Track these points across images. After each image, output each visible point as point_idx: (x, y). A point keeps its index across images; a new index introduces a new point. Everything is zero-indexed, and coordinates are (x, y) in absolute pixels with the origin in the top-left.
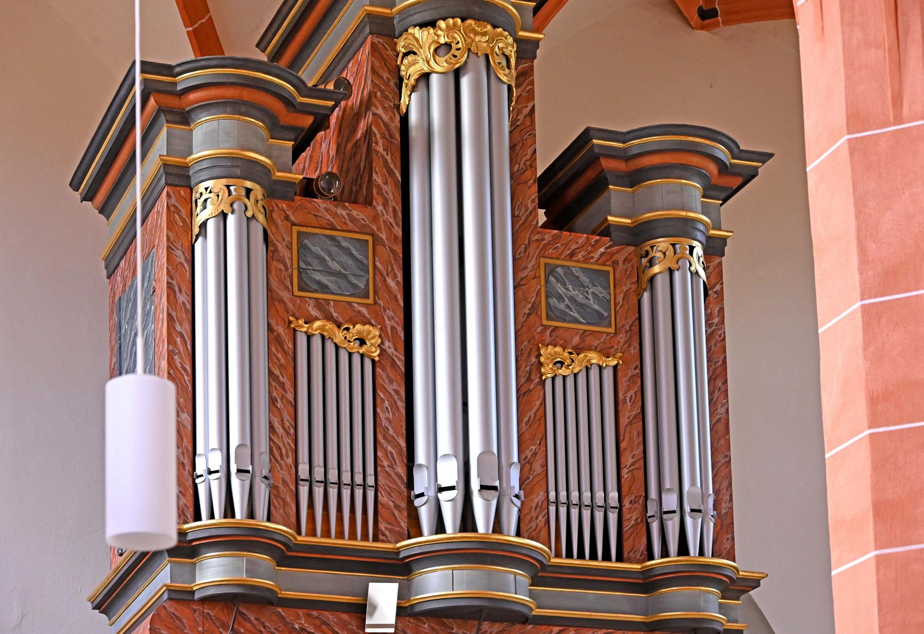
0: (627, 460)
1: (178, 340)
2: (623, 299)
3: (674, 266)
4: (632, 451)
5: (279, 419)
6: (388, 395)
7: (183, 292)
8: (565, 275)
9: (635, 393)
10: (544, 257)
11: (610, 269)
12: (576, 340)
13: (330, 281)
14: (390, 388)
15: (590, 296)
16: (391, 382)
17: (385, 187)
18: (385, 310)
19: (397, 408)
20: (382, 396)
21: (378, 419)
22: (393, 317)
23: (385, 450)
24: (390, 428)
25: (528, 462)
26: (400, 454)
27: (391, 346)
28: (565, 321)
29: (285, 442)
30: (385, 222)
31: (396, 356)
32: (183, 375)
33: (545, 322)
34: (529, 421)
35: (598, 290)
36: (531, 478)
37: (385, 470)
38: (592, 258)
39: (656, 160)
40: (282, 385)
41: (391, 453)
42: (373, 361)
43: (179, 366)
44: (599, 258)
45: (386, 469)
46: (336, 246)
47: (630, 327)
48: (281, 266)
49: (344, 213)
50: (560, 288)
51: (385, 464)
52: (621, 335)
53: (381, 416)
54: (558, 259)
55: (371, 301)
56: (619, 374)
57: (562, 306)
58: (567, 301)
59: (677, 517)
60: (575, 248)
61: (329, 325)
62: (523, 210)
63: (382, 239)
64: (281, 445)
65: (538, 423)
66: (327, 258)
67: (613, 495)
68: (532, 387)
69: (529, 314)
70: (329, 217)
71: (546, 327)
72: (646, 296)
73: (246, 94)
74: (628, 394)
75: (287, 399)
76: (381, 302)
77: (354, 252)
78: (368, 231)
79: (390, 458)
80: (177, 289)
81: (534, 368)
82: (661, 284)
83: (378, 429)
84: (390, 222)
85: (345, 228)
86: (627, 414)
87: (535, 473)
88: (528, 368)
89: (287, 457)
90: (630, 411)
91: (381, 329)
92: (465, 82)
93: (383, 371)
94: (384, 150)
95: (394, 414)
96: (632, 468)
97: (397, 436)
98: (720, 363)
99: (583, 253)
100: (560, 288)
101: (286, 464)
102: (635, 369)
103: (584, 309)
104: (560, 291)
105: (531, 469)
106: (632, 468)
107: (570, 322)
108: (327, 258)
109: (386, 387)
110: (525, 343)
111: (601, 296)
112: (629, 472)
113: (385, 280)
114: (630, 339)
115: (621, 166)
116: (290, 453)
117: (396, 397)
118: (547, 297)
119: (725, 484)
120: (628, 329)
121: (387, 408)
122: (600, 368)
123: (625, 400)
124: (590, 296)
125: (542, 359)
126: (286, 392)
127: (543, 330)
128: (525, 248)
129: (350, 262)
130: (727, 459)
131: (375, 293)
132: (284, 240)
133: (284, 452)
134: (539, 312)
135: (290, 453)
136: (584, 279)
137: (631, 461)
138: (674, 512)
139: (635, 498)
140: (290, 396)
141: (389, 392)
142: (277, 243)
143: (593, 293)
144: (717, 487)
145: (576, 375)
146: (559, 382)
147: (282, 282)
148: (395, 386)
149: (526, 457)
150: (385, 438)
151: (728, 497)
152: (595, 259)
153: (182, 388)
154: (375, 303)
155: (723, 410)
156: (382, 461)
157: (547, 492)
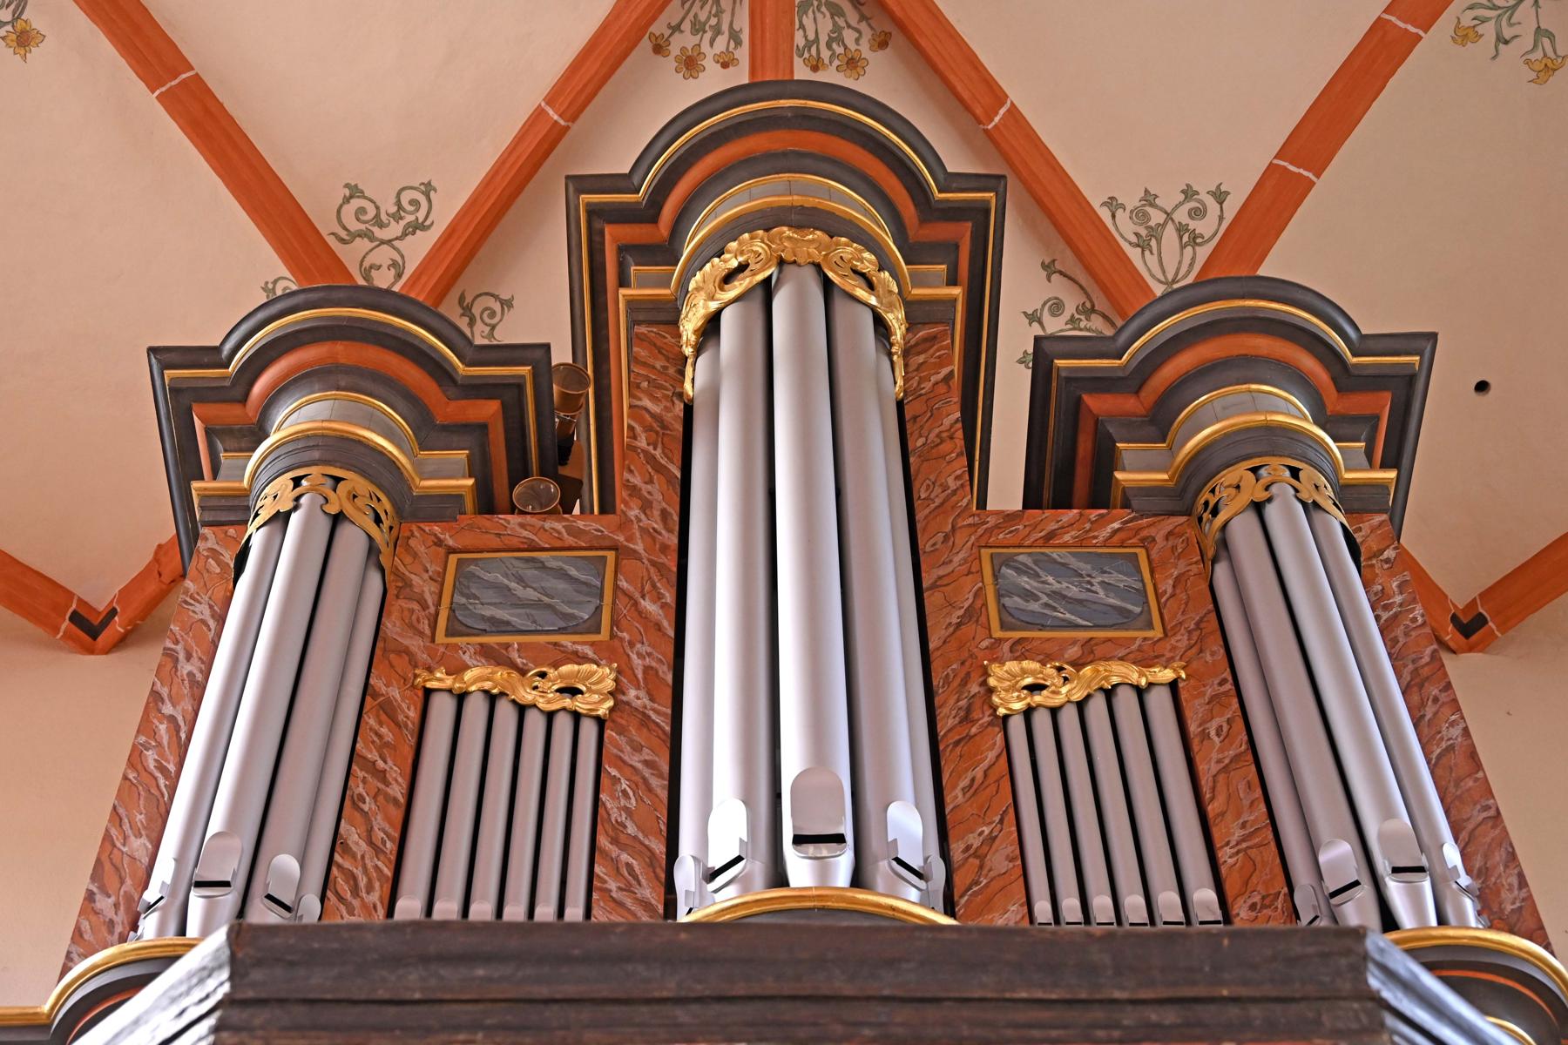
0: (1229, 833)
1: (163, 728)
2: (1174, 586)
3: (1260, 496)
4: (1239, 816)
5: (362, 829)
6: (628, 771)
7: (195, 660)
8: (1037, 565)
9: (1229, 721)
10: (986, 547)
11: (1141, 553)
12: (1073, 652)
13: (512, 615)
14: (635, 760)
15: (1097, 588)
16: (637, 749)
17: (645, 488)
18: (631, 644)
19: (650, 789)
20: (614, 772)
21: (601, 810)
22: (649, 654)
23: (615, 863)
24: (629, 824)
25: (975, 855)
26: (651, 865)
27: (642, 694)
28: (1042, 627)
29: (369, 865)
30: (643, 530)
31: (654, 710)
32: (156, 778)
33: (997, 634)
34: (971, 786)
35: (1116, 578)
36: (985, 882)
37: (614, 900)
38: (1095, 537)
39: (1184, 361)
40: (382, 775)
41: (628, 865)
42: (601, 722)
43: (151, 765)
44: (1111, 537)
45: (614, 895)
46: (536, 568)
47: (1197, 624)
48: (416, 606)
49: (559, 526)
50: (1025, 582)
51: (612, 885)
52: (1178, 637)
53: (609, 806)
54: (1019, 546)
55: (604, 635)
56: (1184, 695)
57: (1034, 606)
58: (1045, 599)
59: (1365, 892)
60: (1054, 528)
61: (501, 673)
62: (938, 490)
63: (635, 551)
64: (358, 872)
65: (993, 788)
66: (513, 585)
67: (1204, 896)
68: (974, 730)
69: (959, 625)
70: (525, 533)
71: (1000, 641)
72: (1221, 572)
73: (342, 351)
74: (1212, 726)
75: (387, 796)
76: (625, 635)
77: (573, 572)
78: (607, 543)
79: (626, 874)
80: (182, 656)
81: (978, 703)
82: (1244, 532)
83: (599, 827)
84: (654, 529)
85: (558, 544)
86: (1215, 756)
87: (992, 874)
88: (963, 703)
89: (370, 889)
90: (1221, 750)
91: (619, 671)
92: (781, 304)
93: (619, 734)
94: (648, 444)
95: (639, 799)
96: (1244, 845)
97: (646, 836)
98: (1426, 659)
99: (1073, 533)
100: (1025, 582)
101: (364, 905)
102: (1221, 684)
103: (1085, 606)
104: (1027, 587)
105: (981, 867)
106: (1244, 845)
107: (1053, 628)
108: (513, 585)
109: (626, 758)
110: (954, 666)
111: (1122, 586)
112: (1238, 853)
113: (636, 604)
114: (1201, 639)
115: (1129, 404)
116: (377, 885)
117: (647, 772)
118: (999, 596)
119: (1499, 856)
120: (1192, 626)
121: (624, 792)
122: (1140, 692)
123: (1205, 735)
124: (1097, 588)
125: (992, 682)
126: (387, 784)
127: (992, 644)
128: (946, 538)
129: (561, 585)
130: (1492, 813)
131: (615, 622)
132: (427, 571)
133: (363, 882)
134: (983, 619)
135: (377, 885)
136: (1084, 567)
137: (1238, 834)
138: (1356, 883)
139: (1263, 898)
140: (398, 791)
141: (631, 766)
142: (413, 576)
143: (1102, 583)
144: (1478, 863)
145: (1081, 706)
146: (1042, 721)
147: (411, 626)
148: (647, 755)
149: (968, 848)
150: (615, 841)
151: (1514, 881)
152: (1101, 539)
153: (146, 798)
154: (613, 636)
155: (1456, 732)
156: (605, 882)
157: (1029, 903)
